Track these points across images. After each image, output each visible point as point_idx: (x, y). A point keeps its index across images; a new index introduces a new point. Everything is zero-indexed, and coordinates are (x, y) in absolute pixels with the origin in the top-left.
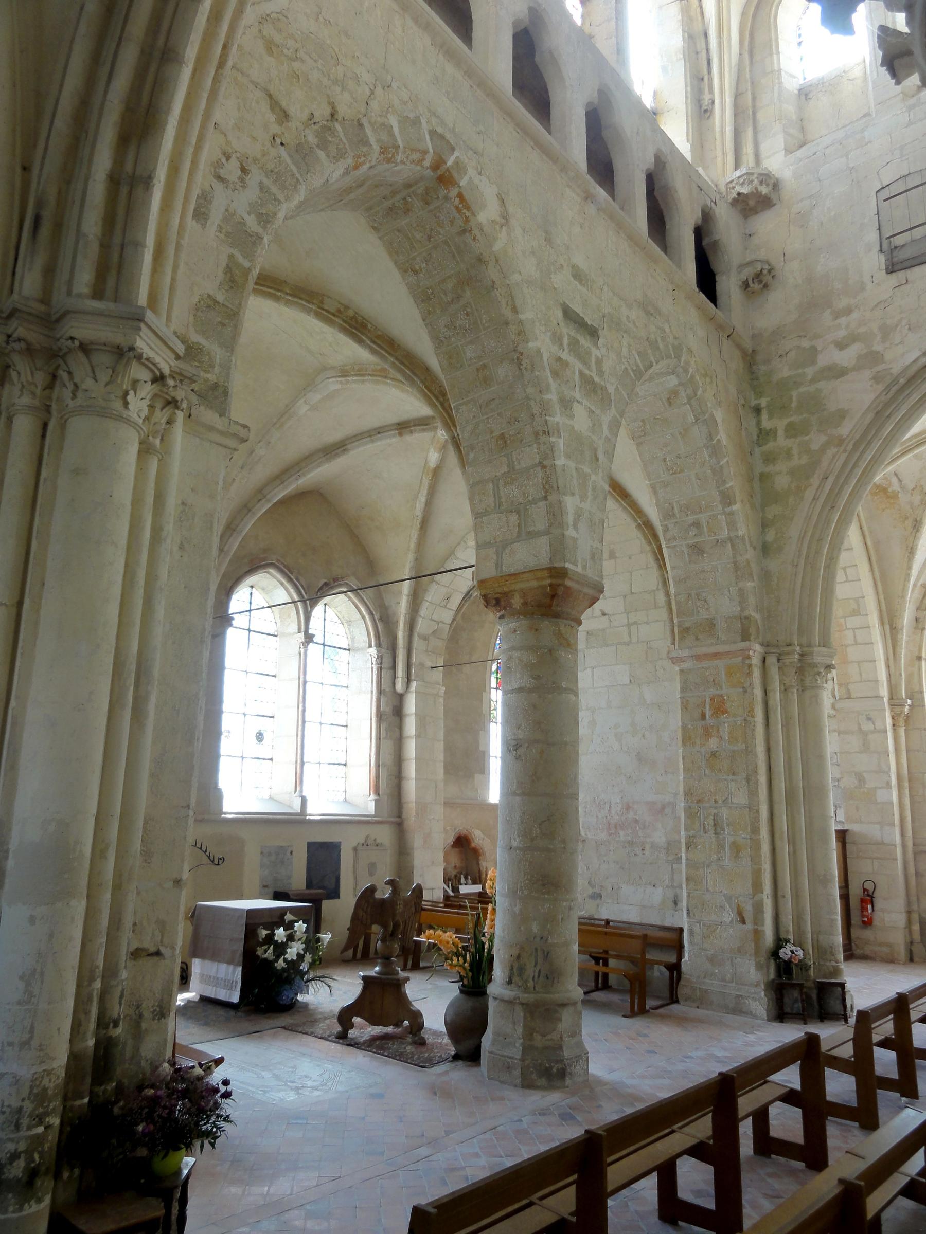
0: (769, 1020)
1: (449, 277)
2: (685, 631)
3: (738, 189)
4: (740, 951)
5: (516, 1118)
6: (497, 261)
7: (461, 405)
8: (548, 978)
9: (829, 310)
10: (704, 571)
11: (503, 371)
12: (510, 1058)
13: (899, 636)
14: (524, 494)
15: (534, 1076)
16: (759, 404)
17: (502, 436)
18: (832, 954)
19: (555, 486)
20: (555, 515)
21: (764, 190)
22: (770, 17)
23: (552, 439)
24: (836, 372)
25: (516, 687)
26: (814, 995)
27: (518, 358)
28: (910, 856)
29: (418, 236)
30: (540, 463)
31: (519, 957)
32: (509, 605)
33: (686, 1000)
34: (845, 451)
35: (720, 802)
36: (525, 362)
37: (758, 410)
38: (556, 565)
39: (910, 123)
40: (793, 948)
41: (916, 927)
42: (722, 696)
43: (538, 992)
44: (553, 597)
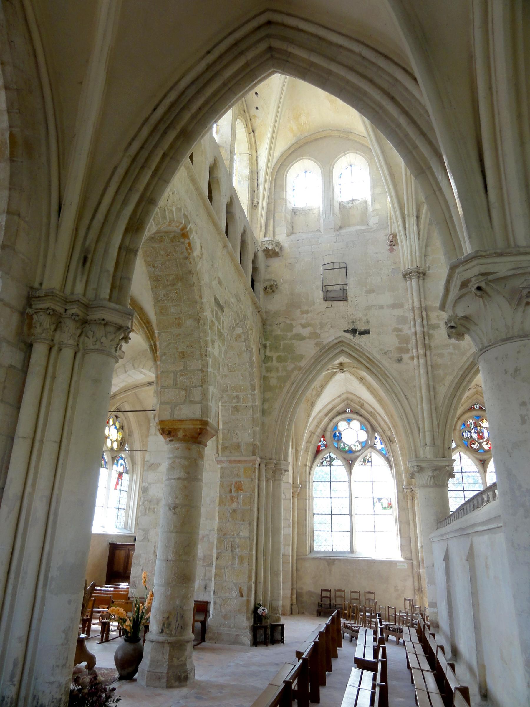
0: (251, 646)
1: (172, 274)
2: (225, 448)
3: (266, 245)
4: (239, 611)
5: (176, 702)
6: (197, 274)
7: (163, 332)
8: (182, 628)
9: (299, 310)
10: (238, 420)
11: (189, 323)
12: (161, 673)
13: (299, 454)
14: (190, 382)
15: (173, 681)
16: (266, 344)
17: (183, 353)
18: (278, 610)
19: (206, 381)
20: (205, 394)
21: (277, 249)
22: (284, 175)
23: (208, 359)
24: (300, 337)
25: (177, 477)
26: (269, 631)
27: (198, 319)
28: (295, 561)
29: (162, 253)
30: (201, 369)
31: (168, 618)
32: (175, 435)
33: (209, 640)
34: (302, 373)
35: (235, 535)
36: (201, 322)
37: (265, 346)
38: (203, 419)
39: (336, 242)
40: (263, 608)
41: (295, 597)
42: (241, 482)
43: (177, 636)
44: (199, 434)
